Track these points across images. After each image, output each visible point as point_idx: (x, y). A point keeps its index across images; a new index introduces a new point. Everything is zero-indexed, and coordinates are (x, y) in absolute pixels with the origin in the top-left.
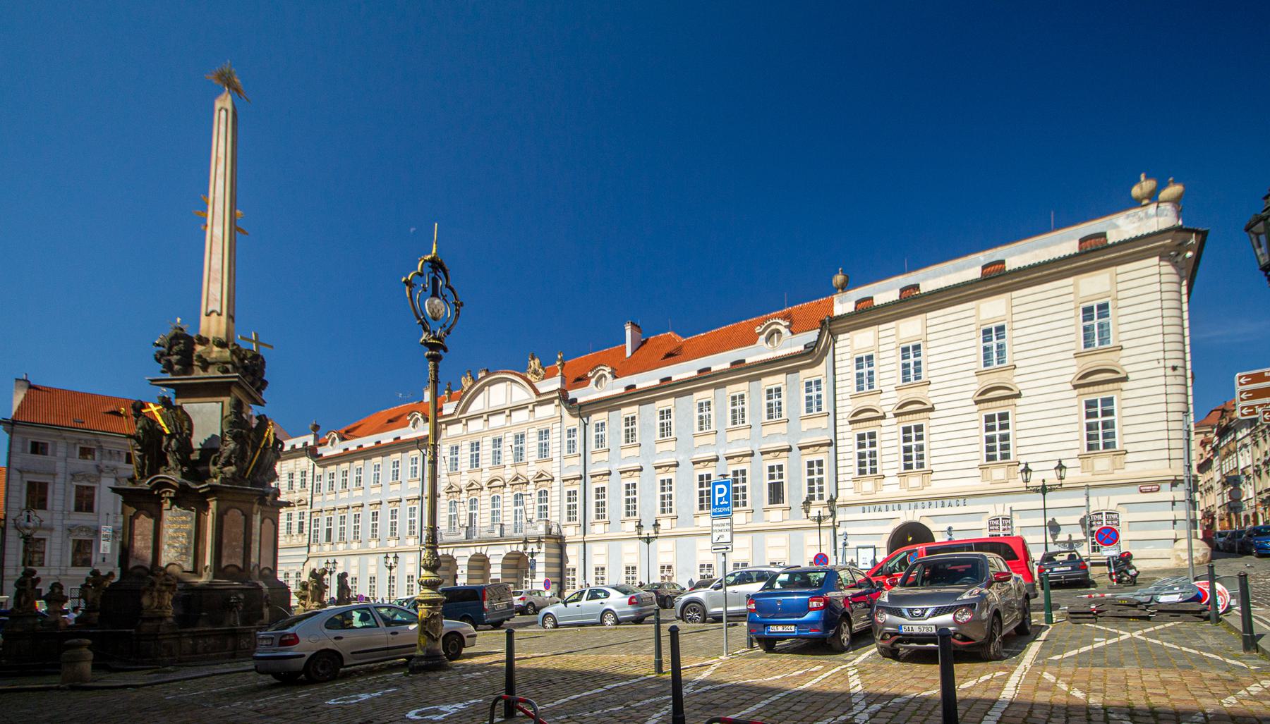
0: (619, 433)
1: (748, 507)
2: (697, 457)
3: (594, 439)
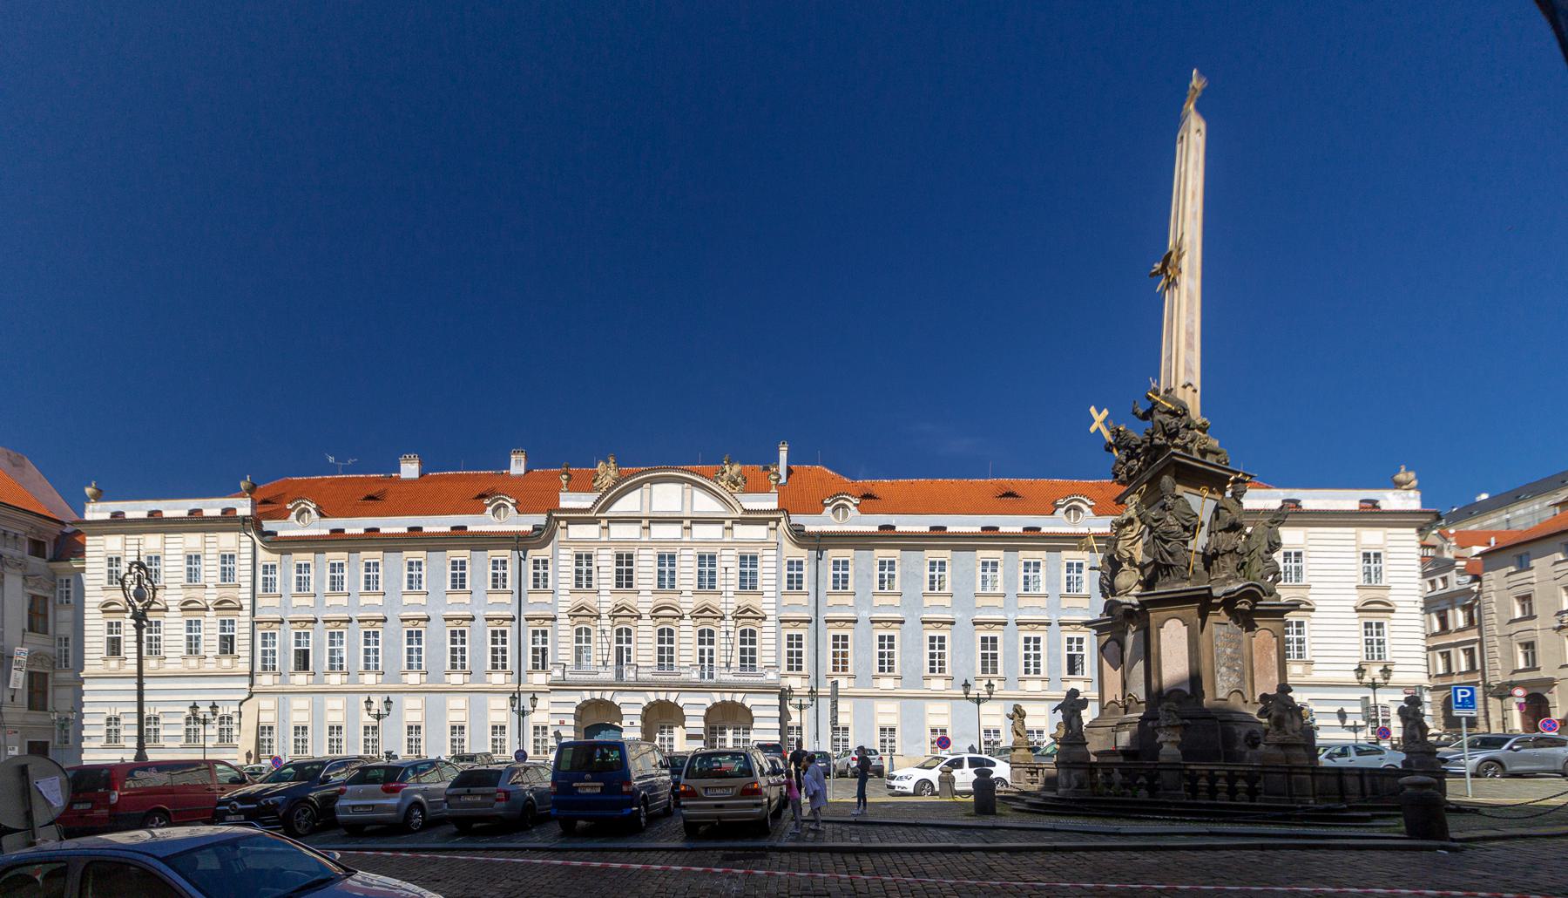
0: (870, 576)
2: (980, 617)
3: (831, 579)
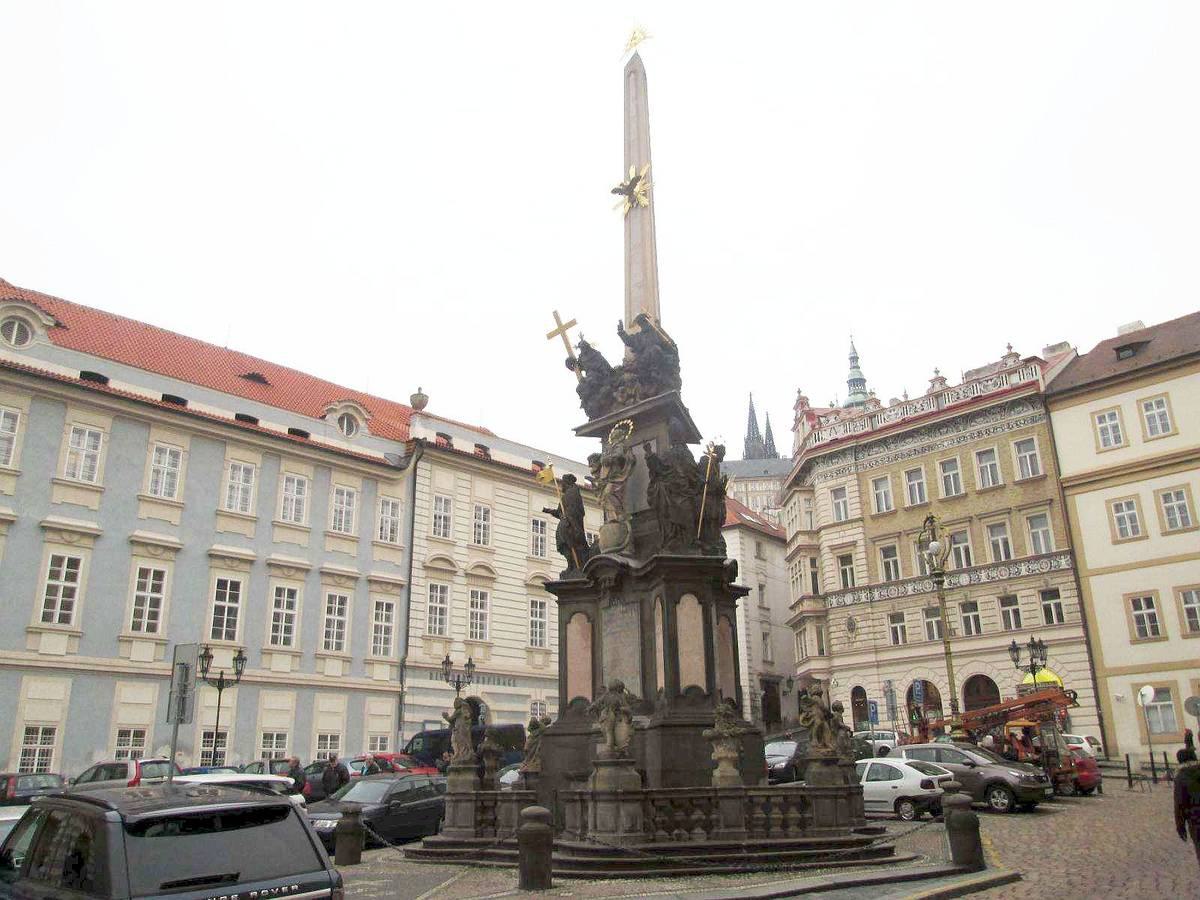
1: (294, 645)
